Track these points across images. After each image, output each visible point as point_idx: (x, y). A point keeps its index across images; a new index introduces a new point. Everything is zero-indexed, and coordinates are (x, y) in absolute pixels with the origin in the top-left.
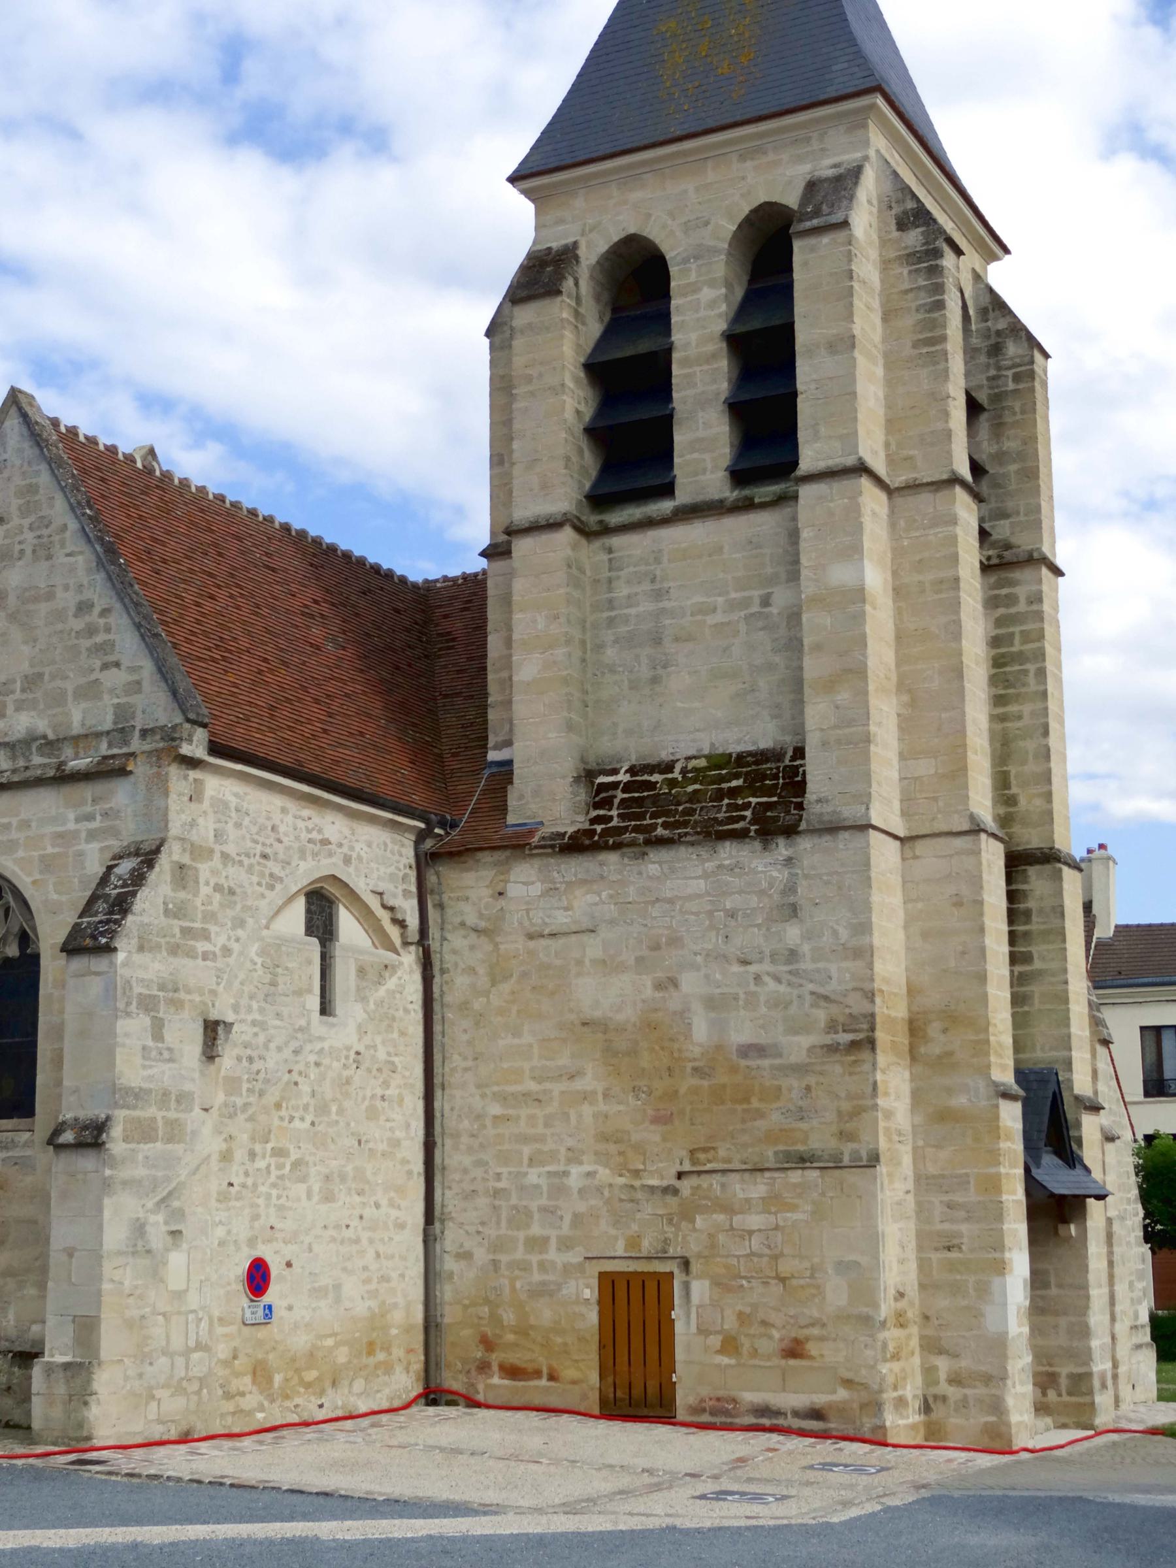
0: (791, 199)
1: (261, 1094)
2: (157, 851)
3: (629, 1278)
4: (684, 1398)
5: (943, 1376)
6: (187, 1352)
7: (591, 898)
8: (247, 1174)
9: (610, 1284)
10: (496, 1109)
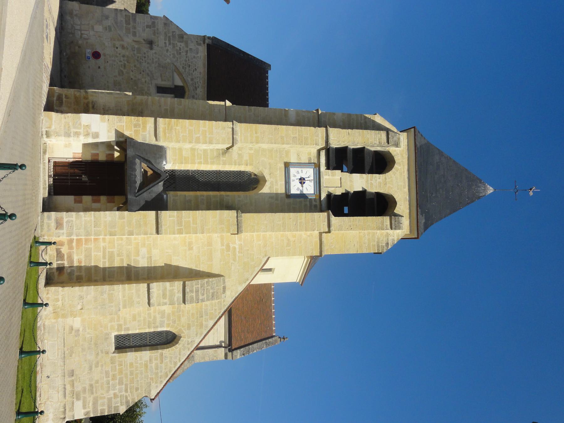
1: (138, 60)
6: (80, 30)
8: (120, 54)
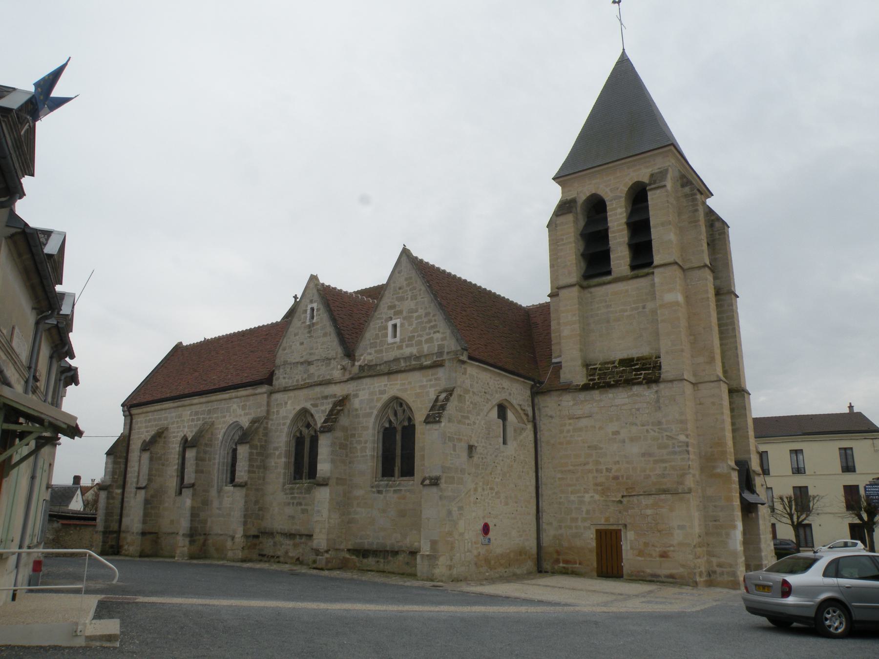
0: (646, 180)
2: (453, 390)
3: (606, 532)
4: (626, 570)
5: (715, 564)
7: (590, 406)
9: (599, 533)
10: (559, 475)
